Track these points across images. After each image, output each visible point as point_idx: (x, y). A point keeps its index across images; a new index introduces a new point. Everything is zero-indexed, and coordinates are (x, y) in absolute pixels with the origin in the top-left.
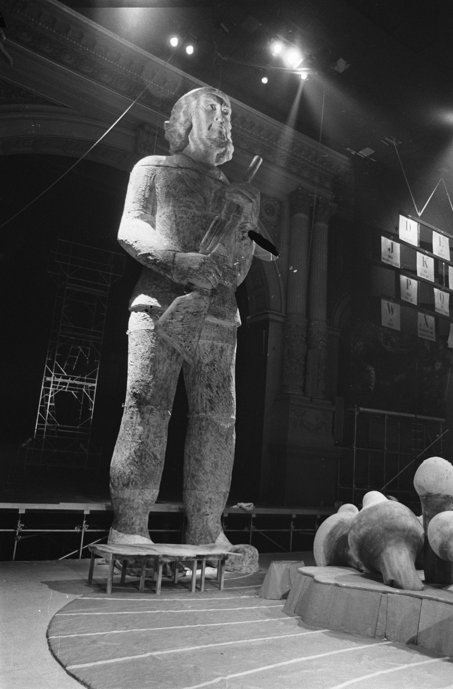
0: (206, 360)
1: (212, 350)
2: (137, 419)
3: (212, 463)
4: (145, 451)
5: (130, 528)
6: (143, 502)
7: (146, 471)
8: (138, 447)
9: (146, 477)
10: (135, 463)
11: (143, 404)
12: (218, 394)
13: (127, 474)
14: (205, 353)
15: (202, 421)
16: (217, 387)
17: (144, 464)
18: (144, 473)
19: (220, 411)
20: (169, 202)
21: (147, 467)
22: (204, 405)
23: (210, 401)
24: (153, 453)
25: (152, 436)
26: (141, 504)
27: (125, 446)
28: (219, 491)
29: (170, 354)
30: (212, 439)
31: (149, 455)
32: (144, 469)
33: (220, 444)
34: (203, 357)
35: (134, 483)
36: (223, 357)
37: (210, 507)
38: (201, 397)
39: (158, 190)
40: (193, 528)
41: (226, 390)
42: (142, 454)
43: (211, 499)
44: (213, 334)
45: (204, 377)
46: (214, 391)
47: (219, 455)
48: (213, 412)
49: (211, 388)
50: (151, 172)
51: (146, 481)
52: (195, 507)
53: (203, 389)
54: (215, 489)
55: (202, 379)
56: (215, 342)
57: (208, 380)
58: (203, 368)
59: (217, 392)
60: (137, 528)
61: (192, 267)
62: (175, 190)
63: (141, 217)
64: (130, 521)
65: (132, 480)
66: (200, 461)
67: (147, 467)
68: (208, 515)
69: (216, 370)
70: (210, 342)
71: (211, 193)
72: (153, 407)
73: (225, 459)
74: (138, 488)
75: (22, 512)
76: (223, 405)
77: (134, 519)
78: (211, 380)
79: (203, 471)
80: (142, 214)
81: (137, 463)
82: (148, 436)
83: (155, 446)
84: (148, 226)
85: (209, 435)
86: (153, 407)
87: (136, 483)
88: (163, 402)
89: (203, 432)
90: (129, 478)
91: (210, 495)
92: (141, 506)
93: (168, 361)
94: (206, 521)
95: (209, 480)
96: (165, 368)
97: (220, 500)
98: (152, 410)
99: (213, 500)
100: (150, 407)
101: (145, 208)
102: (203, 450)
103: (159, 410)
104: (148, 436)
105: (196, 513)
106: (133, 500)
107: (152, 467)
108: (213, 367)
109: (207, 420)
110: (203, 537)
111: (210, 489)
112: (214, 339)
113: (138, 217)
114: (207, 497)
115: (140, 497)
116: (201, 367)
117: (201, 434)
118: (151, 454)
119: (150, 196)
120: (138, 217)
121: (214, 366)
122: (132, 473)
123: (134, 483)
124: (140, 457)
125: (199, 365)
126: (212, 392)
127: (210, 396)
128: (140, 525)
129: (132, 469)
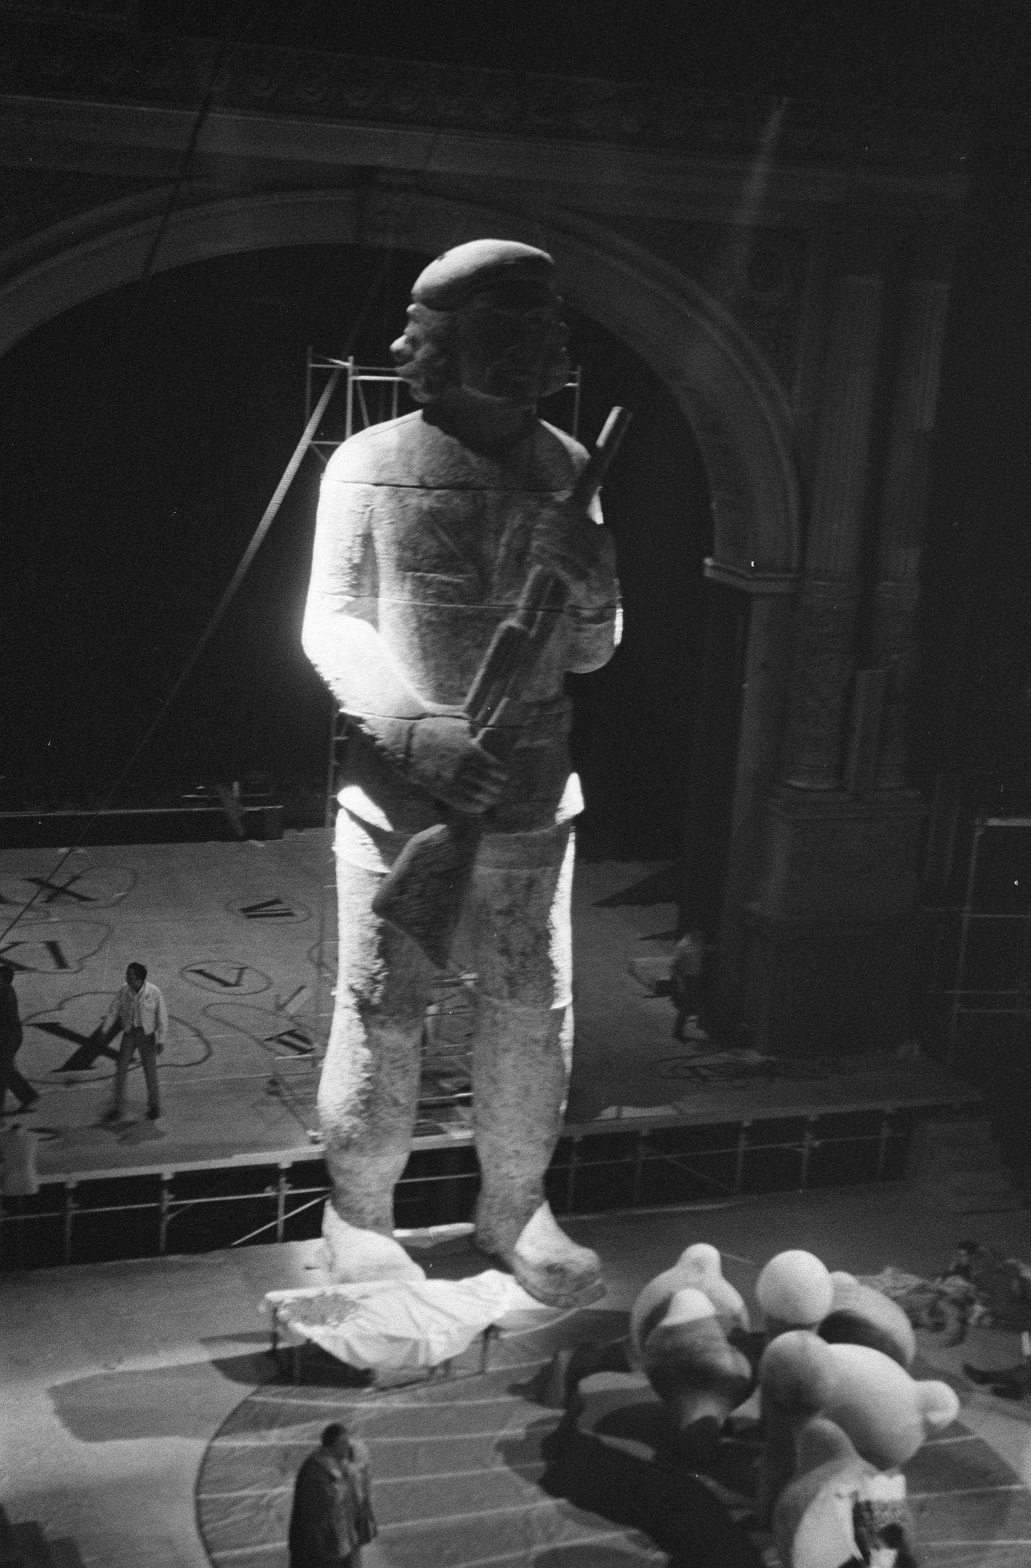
0: (498, 905)
1: (509, 886)
2: (358, 1033)
20: (404, 578)
25: (386, 1067)
39: (380, 546)
50: (363, 502)
60: (371, 1218)
62: (416, 554)
63: (349, 609)
70: (503, 871)
71: (497, 546)
75: (167, 1176)
80: (349, 604)
82: (379, 1069)
83: (393, 1084)
84: (364, 625)
88: (405, 1007)
101: (356, 586)
103: (397, 1022)
113: (341, 611)
119: (364, 558)
120: (341, 611)
124: (367, 1103)
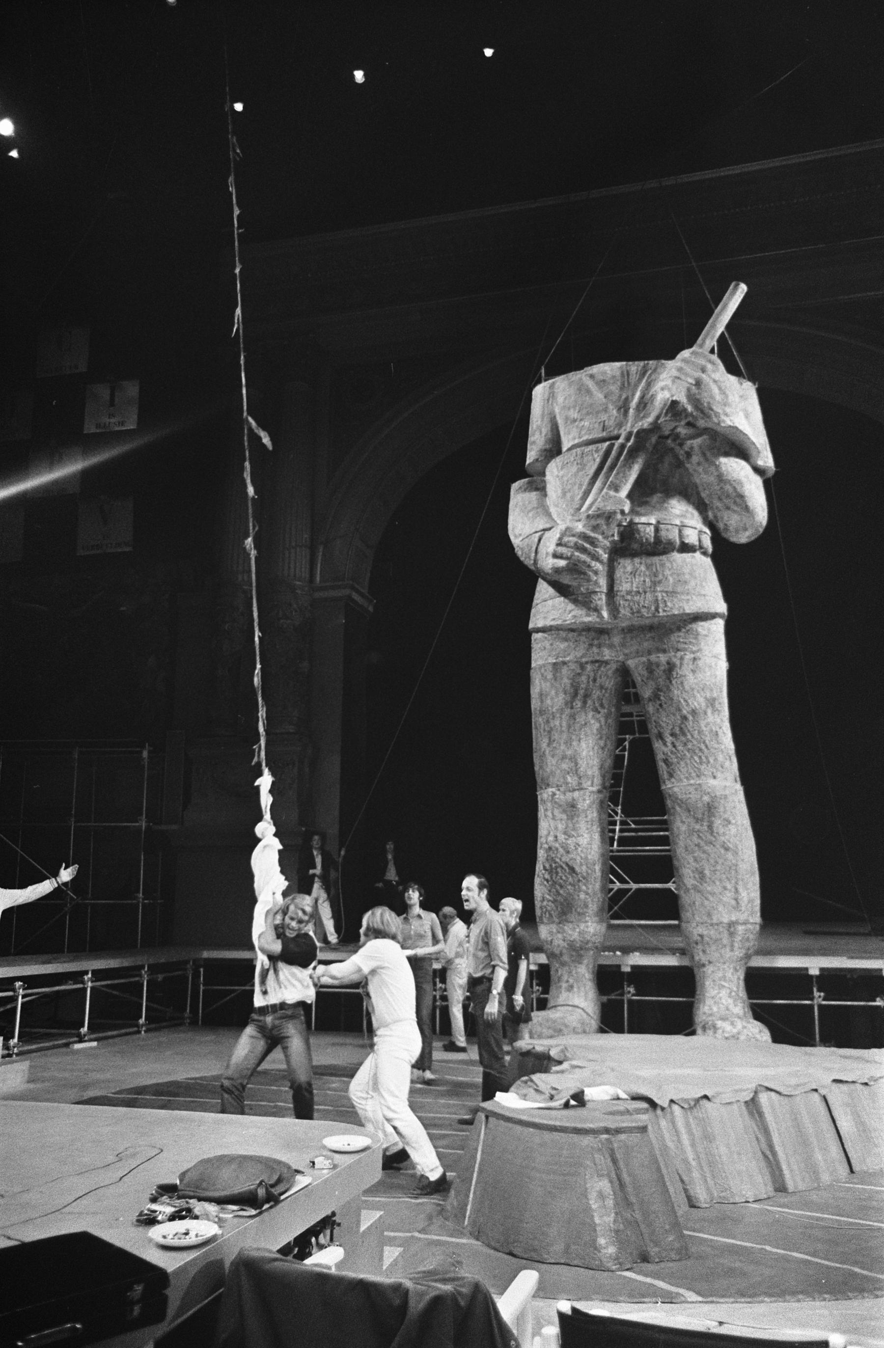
3: (693, 872)
4: (555, 863)
6: (565, 945)
9: (562, 904)
12: (674, 746)
16: (672, 735)
18: (559, 898)
19: (682, 777)
23: (666, 761)
24: (567, 865)
26: (564, 947)
28: (715, 921)
29: (568, 698)
32: (557, 891)
33: (699, 837)
36: (674, 682)
37: (704, 951)
41: (689, 737)
42: (551, 866)
43: (701, 936)
44: (646, 644)
46: (669, 744)
47: (703, 856)
48: (673, 780)
54: (705, 918)
56: (653, 658)
59: (673, 743)
67: (561, 887)
69: (665, 706)
70: (644, 659)
73: (717, 862)
74: (553, 922)
76: (687, 764)
77: (560, 973)
78: (660, 725)
81: (547, 881)
86: (554, 790)
87: (551, 915)
91: (701, 930)
92: (564, 951)
93: (568, 711)
95: (694, 903)
96: (564, 724)
97: (718, 936)
98: (554, 794)
104: (556, 837)
107: (569, 887)
108: (658, 702)
112: (649, 653)
115: (560, 936)
121: (659, 699)
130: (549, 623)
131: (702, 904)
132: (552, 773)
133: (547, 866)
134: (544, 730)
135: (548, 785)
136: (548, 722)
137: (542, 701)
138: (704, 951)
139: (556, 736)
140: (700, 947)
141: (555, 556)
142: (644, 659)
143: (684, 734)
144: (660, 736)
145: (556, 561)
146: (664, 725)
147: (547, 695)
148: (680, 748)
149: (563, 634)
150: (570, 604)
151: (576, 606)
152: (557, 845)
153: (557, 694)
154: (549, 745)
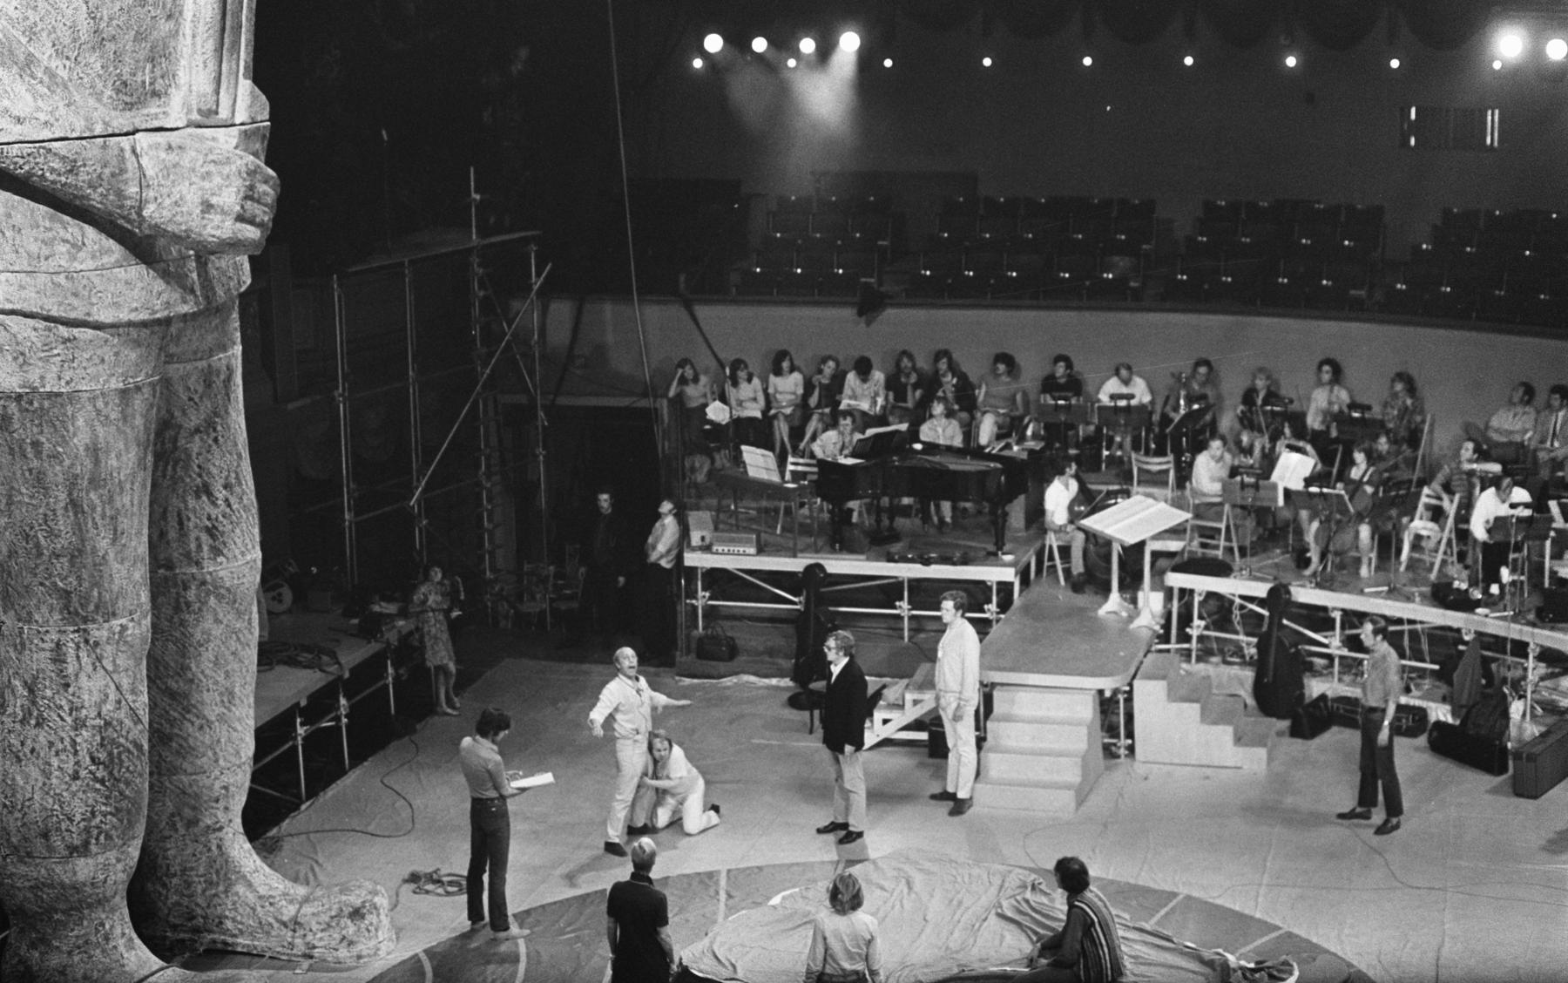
3: (221, 694)
4: (119, 745)
5: (103, 951)
7: (126, 797)
8: (98, 738)
9: (129, 812)
10: (98, 786)
11: (94, 621)
13: (78, 818)
14: (191, 399)
15: (186, 588)
16: (225, 487)
17: (118, 780)
18: (124, 804)
19: (237, 552)
21: (128, 783)
22: (193, 546)
27: (51, 744)
30: (217, 631)
31: (129, 751)
32: (121, 793)
34: (184, 413)
35: (102, 837)
38: (181, 523)
40: (176, 868)
42: (110, 754)
43: (226, 788)
45: (187, 467)
49: (209, 494)
51: (129, 821)
52: (177, 819)
53: (185, 502)
54: (233, 759)
55: (180, 472)
57: (200, 476)
58: (181, 442)
61: (214, 200)
64: (97, 931)
65: (95, 832)
66: (186, 696)
67: (128, 783)
68: (221, 829)
72: (124, 621)
78: (209, 473)
79: (198, 722)
81: (102, 782)
85: (208, 623)
86: (124, 621)
87: (108, 837)
89: (190, 618)
90: (87, 830)
94: (219, 847)
98: (124, 628)
99: (232, 789)
100: (116, 623)
102: (193, 666)
105: (182, 831)
106: (105, 881)
109: (204, 583)
110: (221, 888)
111: (221, 762)
112: (211, 353)
114: (217, 785)
115: (120, 866)
116: (175, 440)
117: (183, 623)
118: (131, 747)
122: (93, 813)
123: (102, 837)
125: (170, 433)
126: (214, 504)
127: (209, 518)
128: (123, 934)
129: (90, 802)
130: (124, 316)
131: (229, 740)
132: (121, 593)
133: (102, 756)
134: (103, 517)
135: (114, 615)
136: (111, 500)
137: (97, 462)
138: (226, 808)
139: (124, 523)
140: (221, 805)
141: (240, 218)
142: (202, 364)
143: (240, 484)
144: (206, 490)
145: (239, 225)
146: (215, 471)
147: (107, 452)
148: (235, 507)
149: (134, 332)
150: (159, 281)
151: (168, 283)
152: (122, 714)
153: (127, 450)
154: (114, 540)
